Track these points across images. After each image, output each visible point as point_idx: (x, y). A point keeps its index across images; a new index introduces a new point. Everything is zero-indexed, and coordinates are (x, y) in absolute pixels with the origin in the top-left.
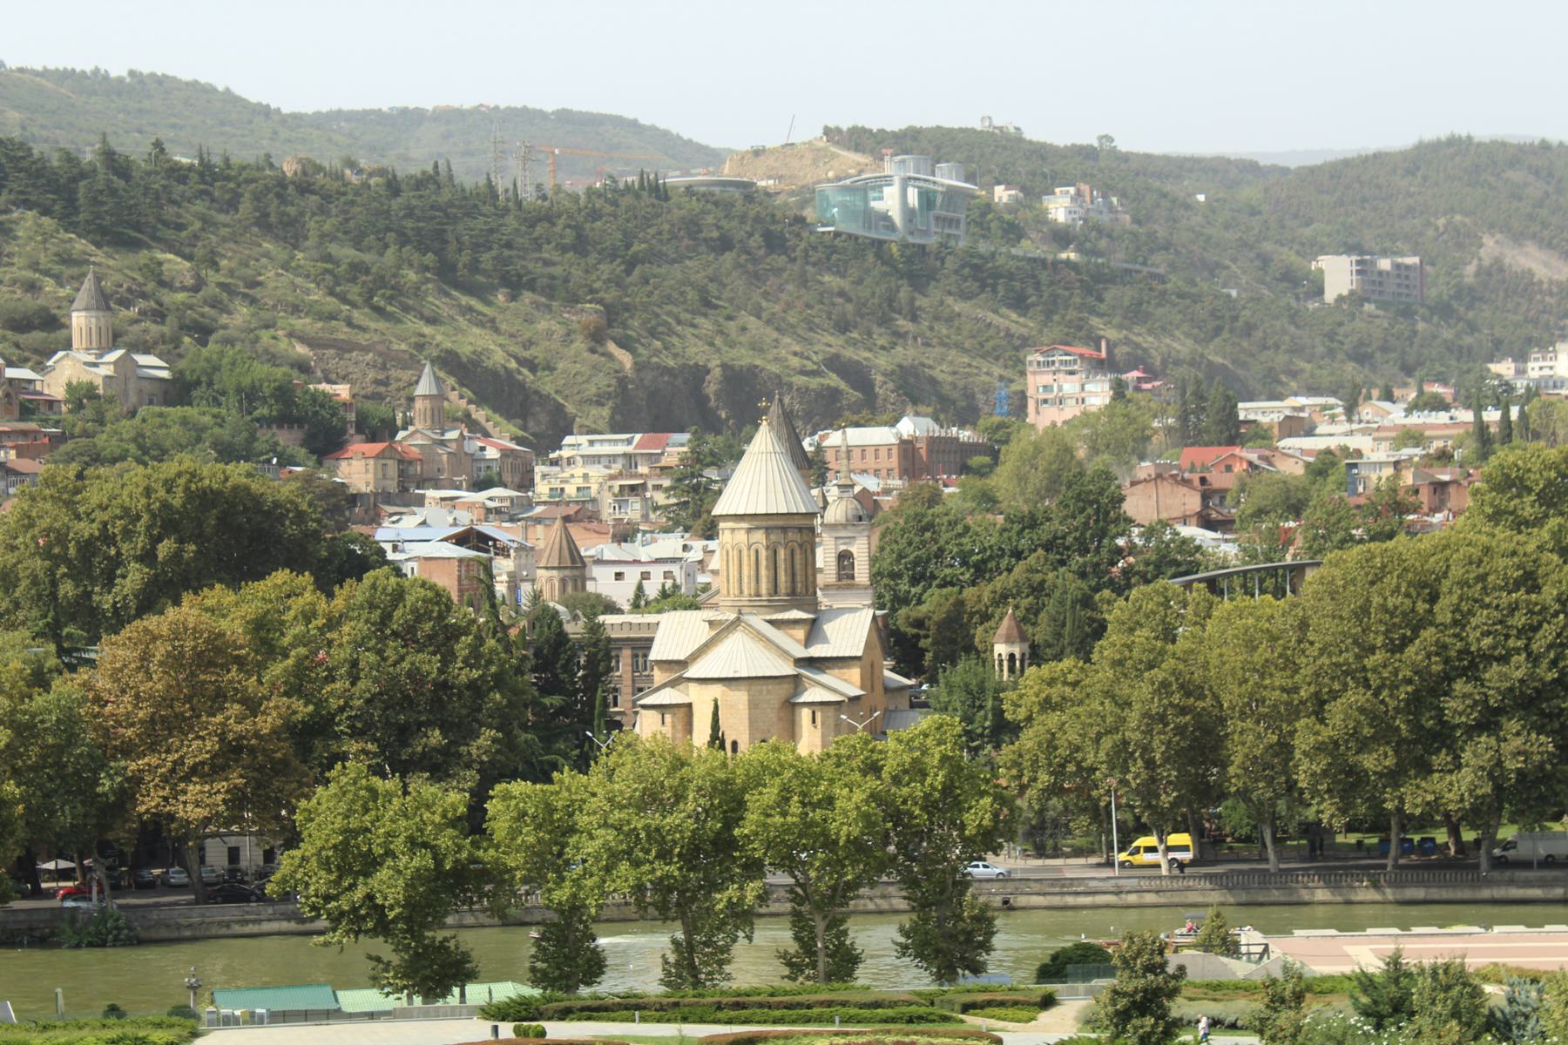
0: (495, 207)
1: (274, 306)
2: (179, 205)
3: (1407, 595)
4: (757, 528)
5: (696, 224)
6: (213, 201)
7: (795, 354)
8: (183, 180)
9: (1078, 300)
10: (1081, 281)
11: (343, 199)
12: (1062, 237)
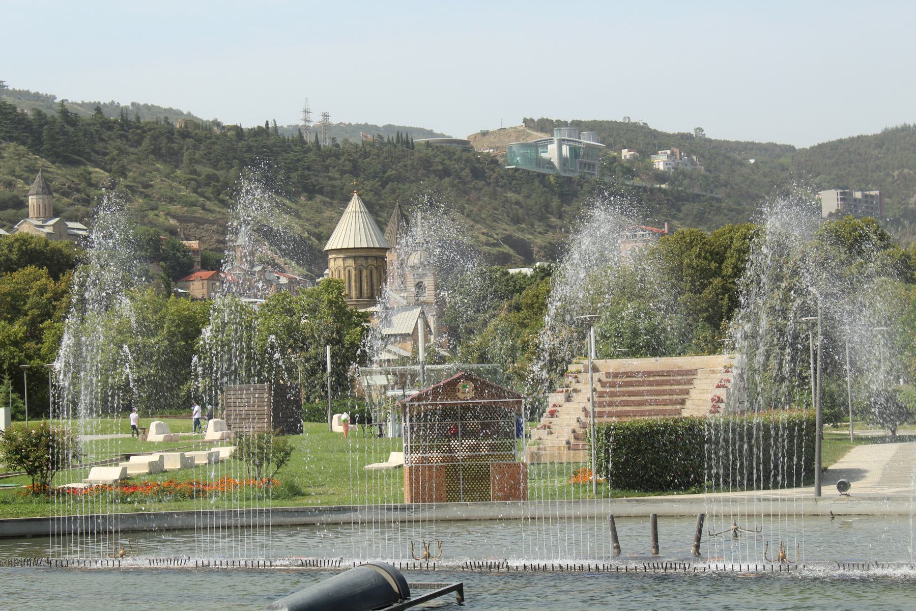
0: (303, 148)
1: (159, 199)
2: (107, 143)
3: (705, 258)
4: (349, 257)
5: (429, 162)
6: (128, 141)
7: (483, 234)
8: (110, 128)
9: (665, 210)
10: (668, 200)
11: (208, 141)
12: (661, 177)
